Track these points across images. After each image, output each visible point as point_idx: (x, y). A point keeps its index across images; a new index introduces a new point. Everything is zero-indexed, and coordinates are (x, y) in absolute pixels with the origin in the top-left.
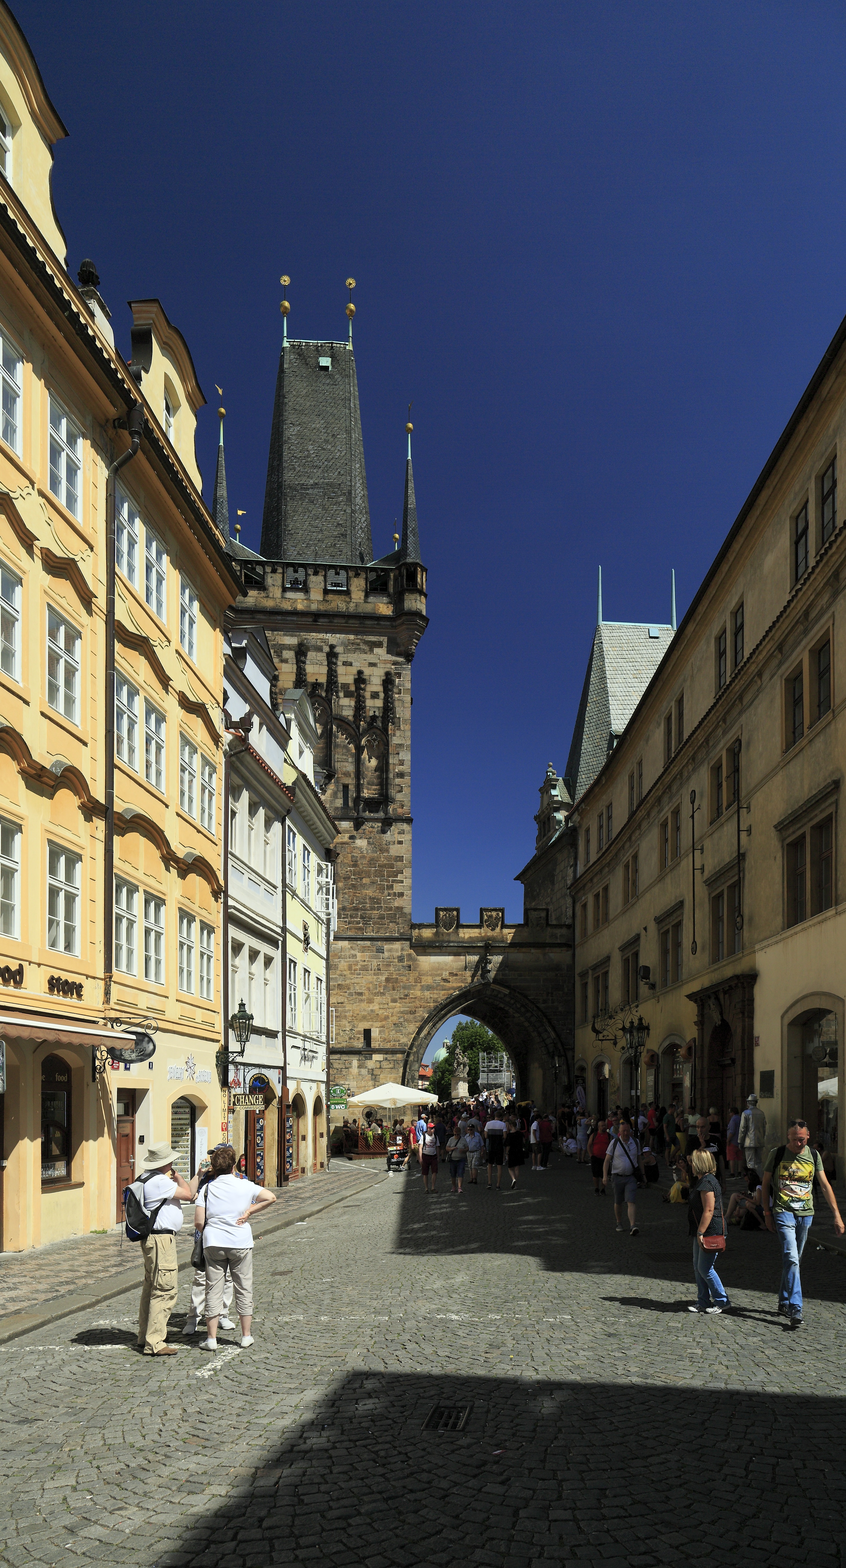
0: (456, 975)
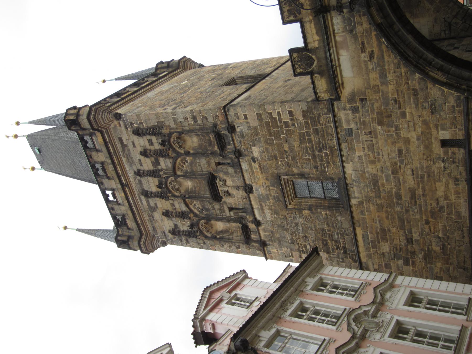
0: (363, 43)
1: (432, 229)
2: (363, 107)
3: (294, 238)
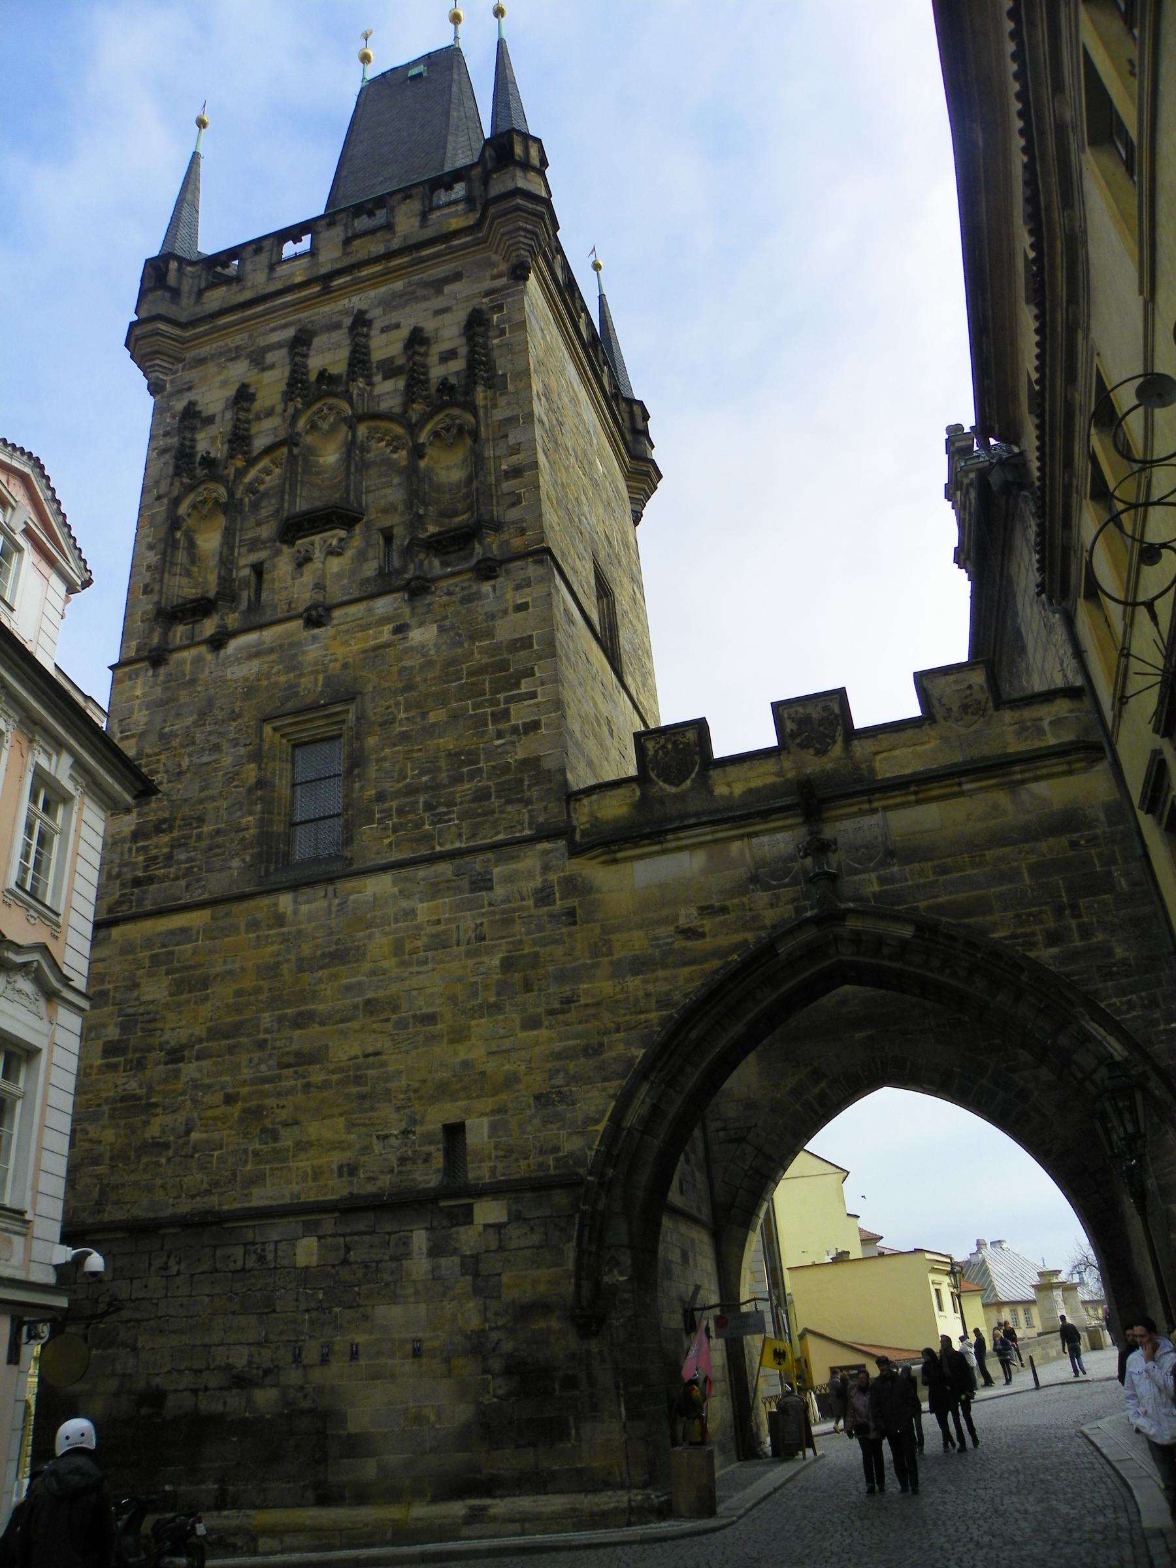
0: (724, 910)
1: (210, 1113)
2: (551, 916)
3: (176, 742)
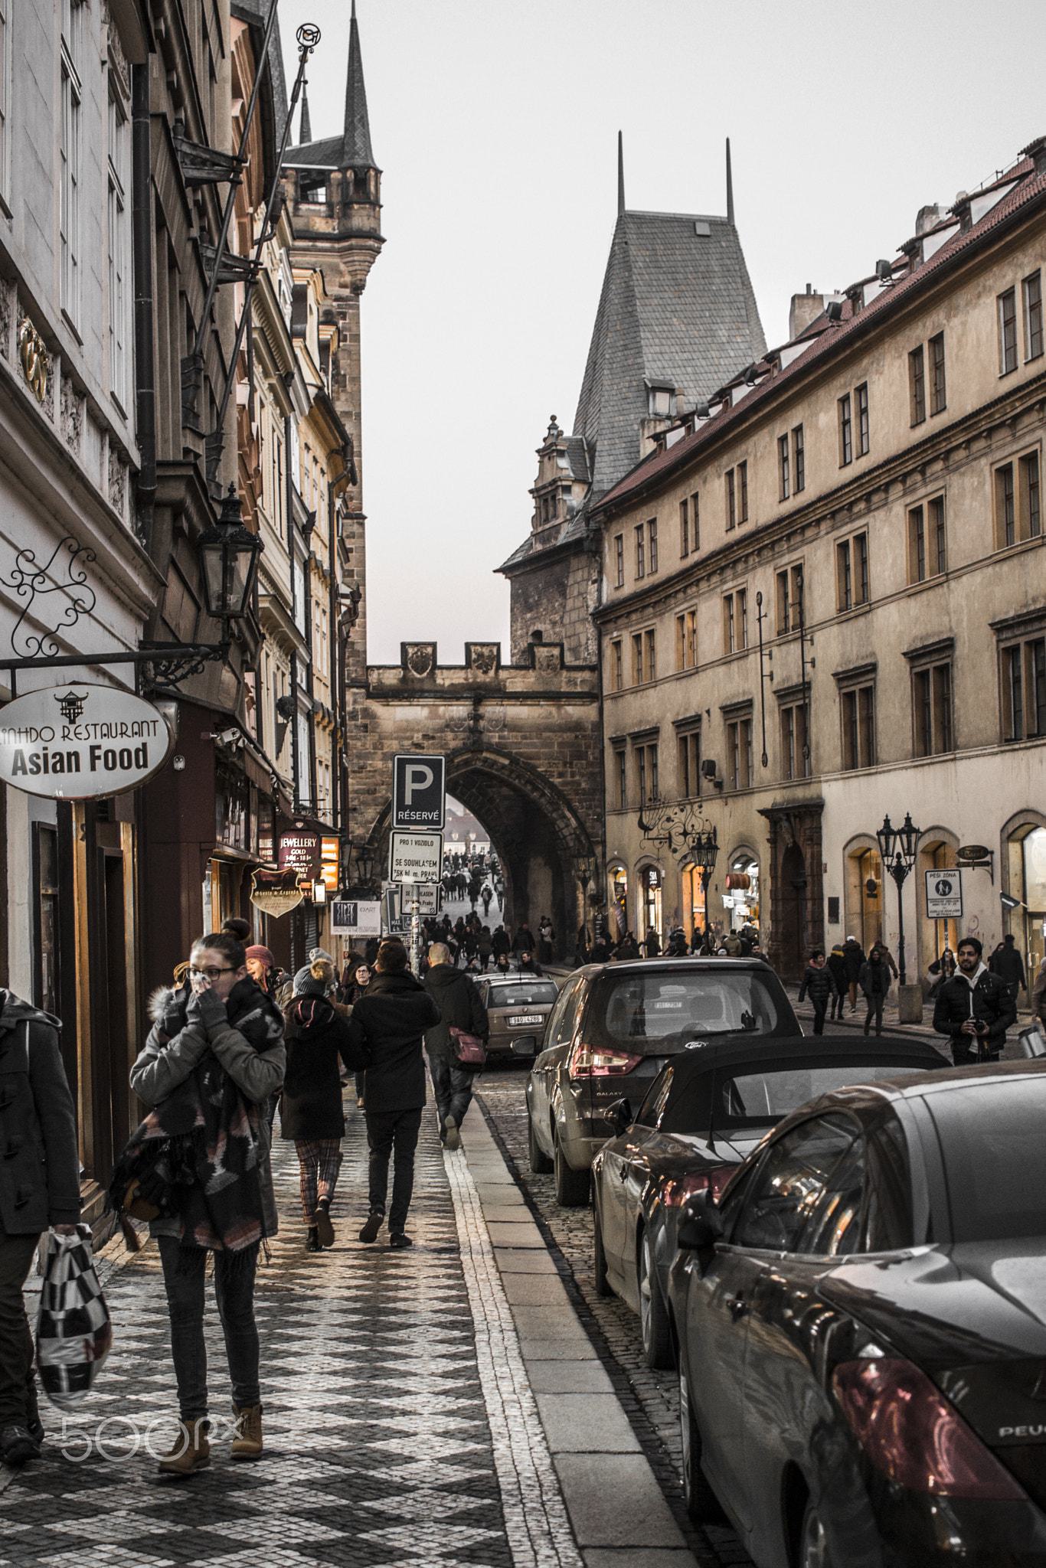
0: (433, 738)
2: (356, 726)
